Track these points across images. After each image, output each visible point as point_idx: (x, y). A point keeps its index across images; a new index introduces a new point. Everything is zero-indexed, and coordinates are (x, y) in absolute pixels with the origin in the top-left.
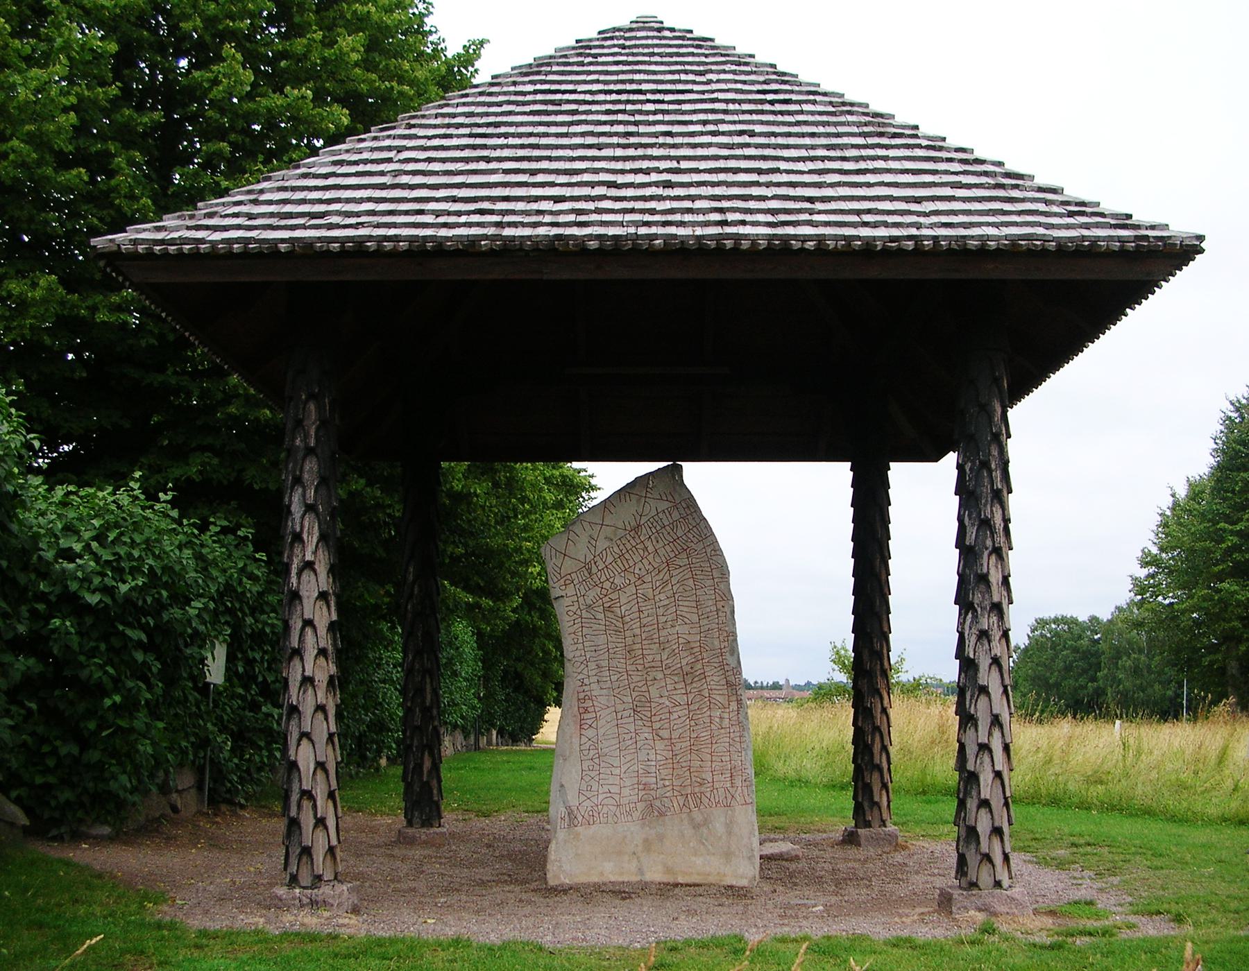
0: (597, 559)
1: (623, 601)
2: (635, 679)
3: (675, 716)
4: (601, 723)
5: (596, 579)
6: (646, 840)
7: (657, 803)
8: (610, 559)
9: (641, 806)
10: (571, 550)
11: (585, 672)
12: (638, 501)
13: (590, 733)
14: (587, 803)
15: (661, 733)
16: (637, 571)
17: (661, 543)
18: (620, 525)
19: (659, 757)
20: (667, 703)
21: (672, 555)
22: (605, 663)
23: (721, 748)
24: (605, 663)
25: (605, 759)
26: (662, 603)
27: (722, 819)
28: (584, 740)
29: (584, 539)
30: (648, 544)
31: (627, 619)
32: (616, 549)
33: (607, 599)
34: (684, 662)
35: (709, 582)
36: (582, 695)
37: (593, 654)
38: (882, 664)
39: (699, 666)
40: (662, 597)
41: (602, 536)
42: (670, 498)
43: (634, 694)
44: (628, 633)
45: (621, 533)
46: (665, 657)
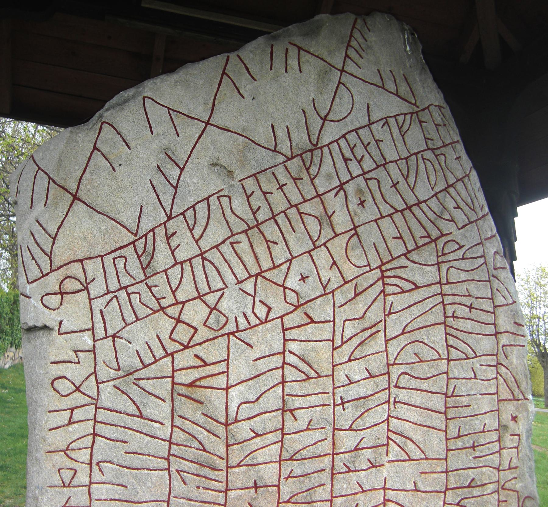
1: (240, 369)
5: (163, 290)
8: (216, 233)
10: (99, 185)
12: (323, 76)
16: (293, 282)
18: (262, 134)
21: (398, 249)
26: (353, 392)
29: (145, 154)
30: (335, 203)
31: (243, 430)
32: (239, 204)
33: (185, 359)
35: (486, 345)
40: (357, 371)
42: (403, 89)
45: (266, 159)
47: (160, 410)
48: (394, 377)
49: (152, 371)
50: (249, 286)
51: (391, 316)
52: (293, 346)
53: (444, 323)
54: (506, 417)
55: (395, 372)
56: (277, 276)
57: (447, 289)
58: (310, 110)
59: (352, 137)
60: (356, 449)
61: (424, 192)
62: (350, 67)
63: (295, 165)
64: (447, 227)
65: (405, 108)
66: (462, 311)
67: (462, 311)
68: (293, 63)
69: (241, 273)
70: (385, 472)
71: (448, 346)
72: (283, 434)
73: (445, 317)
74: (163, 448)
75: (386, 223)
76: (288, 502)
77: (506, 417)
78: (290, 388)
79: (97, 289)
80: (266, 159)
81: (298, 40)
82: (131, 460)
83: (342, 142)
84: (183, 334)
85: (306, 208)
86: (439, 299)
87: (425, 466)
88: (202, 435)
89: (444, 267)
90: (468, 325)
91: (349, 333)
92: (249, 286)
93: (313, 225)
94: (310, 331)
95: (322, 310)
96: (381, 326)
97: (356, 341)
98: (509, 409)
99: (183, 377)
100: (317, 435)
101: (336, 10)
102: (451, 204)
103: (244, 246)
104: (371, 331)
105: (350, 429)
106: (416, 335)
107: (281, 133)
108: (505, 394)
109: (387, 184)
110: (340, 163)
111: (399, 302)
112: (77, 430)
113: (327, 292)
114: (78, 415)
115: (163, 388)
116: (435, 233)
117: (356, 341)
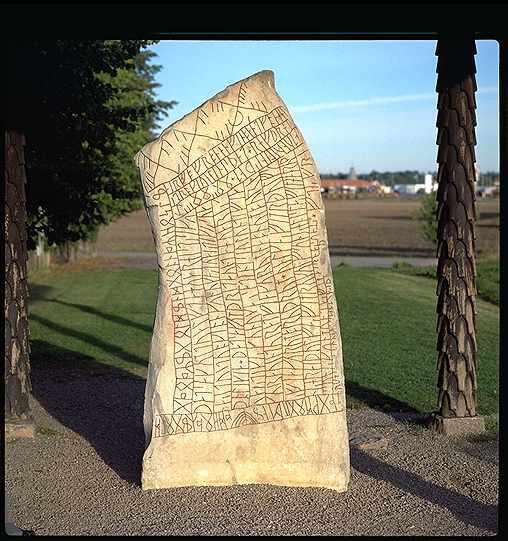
1: (217, 209)
2: (229, 287)
3: (268, 323)
4: (194, 332)
6: (239, 448)
7: (249, 411)
9: (234, 414)
11: (179, 280)
13: (185, 341)
14: (182, 411)
15: (253, 341)
17: (253, 153)
19: (252, 365)
20: (260, 312)
22: (198, 272)
23: (313, 355)
24: (198, 272)
25: (200, 367)
26: (254, 213)
27: (313, 426)
28: (178, 348)
29: (178, 147)
30: (240, 153)
31: (220, 229)
32: (209, 158)
33: (199, 209)
34: (276, 270)
35: (301, 192)
36: (176, 304)
37: (187, 263)
38: (467, 252)
39: (290, 274)
40: (254, 206)
41: (195, 146)
42: (262, 107)
43: (227, 303)
44: (221, 243)
45: (215, 143)
49: (190, 214)
50: (215, 184)
54: (310, 216)
55: (268, 205)
56: (224, 180)
57: (284, 175)
58: (229, 126)
59: (244, 130)
61: (271, 143)
65: (263, 114)
66: (290, 182)
68: (220, 108)
74: (197, 237)
75: (259, 157)
77: (310, 216)
79: (170, 191)
80: (215, 143)
82: (190, 242)
84: (197, 201)
87: (284, 234)
88: (208, 231)
91: (251, 193)
92: (215, 184)
94: (237, 196)
95: (240, 188)
98: (311, 213)
106: (276, 192)
107: (220, 134)
108: (309, 207)
109: (258, 143)
110: (240, 139)
111: (267, 182)
112: (170, 235)
114: (170, 230)
115: (194, 219)
116: (277, 157)
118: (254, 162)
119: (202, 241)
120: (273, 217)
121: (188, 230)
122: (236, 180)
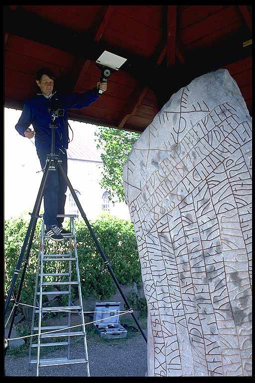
0: (148, 184)
1: (172, 226)
12: (175, 118)
17: (198, 160)
26: (205, 227)
31: (176, 245)
40: (205, 219)
42: (203, 107)
44: (179, 260)
46: (212, 289)
47: (157, 241)
48: (219, 218)
51: (214, 196)
52: (183, 214)
53: (233, 194)
55: (219, 217)
57: (231, 180)
60: (211, 247)
62: (183, 110)
63: (172, 153)
64: (226, 155)
66: (238, 187)
67: (238, 187)
68: (166, 119)
69: (166, 194)
70: (222, 255)
71: (236, 203)
72: (187, 244)
73: (233, 191)
74: (160, 253)
76: (193, 267)
78: (186, 229)
81: (165, 110)
83: (185, 139)
85: (178, 166)
86: (229, 185)
89: (228, 172)
90: (241, 193)
93: (181, 171)
96: (210, 201)
97: (202, 209)
99: (160, 230)
100: (196, 244)
101: (176, 91)
102: (226, 145)
103: (164, 186)
104: (205, 202)
105: (207, 240)
111: (215, 190)
113: (190, 193)
115: (156, 234)
116: (222, 160)
117: (202, 209)
118: (200, 168)
119: (165, 258)
120: (225, 232)
121: (153, 246)
122: (185, 191)
